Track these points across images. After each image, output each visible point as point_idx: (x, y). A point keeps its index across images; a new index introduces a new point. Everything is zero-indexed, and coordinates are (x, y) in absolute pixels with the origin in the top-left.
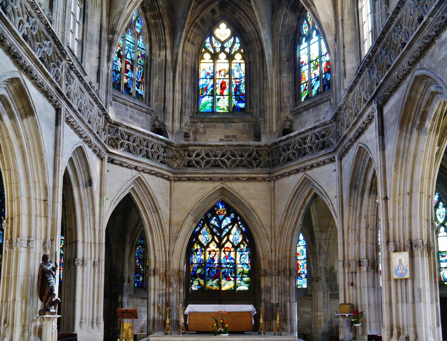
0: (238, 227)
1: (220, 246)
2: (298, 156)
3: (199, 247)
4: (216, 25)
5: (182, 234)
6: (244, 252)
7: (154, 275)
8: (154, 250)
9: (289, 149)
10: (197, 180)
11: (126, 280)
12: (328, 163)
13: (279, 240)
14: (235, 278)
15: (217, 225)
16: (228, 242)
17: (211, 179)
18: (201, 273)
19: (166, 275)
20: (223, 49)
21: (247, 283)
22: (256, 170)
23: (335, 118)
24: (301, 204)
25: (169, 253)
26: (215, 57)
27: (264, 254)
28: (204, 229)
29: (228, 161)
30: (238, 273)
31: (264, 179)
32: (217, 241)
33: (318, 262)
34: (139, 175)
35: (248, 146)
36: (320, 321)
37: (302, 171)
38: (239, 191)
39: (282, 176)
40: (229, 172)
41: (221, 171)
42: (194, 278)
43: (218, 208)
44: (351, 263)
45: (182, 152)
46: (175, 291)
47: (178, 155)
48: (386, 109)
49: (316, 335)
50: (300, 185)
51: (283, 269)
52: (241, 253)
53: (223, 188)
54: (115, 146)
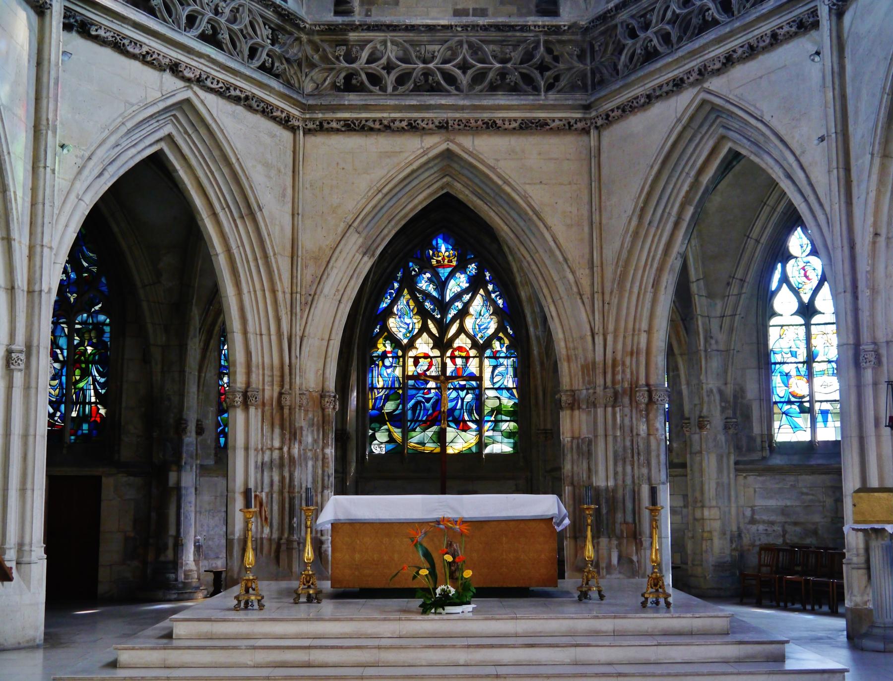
0: (488, 298)
1: (442, 344)
2: (680, 39)
3: (389, 348)
5: (330, 286)
6: (501, 360)
7: (246, 405)
8: (245, 333)
9: (646, 26)
10: (371, 129)
11: (192, 427)
12: (790, 37)
13: (615, 301)
14: (480, 423)
15: (435, 294)
16: (463, 336)
17: (413, 128)
18: (394, 411)
19: (281, 407)
21: (510, 435)
22: (546, 99)
24: (686, 187)
25: (291, 343)
27: (571, 345)
28: (402, 304)
29: (464, 73)
30: (487, 410)
31: (570, 126)
32: (434, 330)
33: (702, 377)
34: (188, 94)
35: (524, 28)
36: (710, 532)
37: (692, 85)
38: (498, 160)
39: (624, 111)
40: (466, 102)
41: (443, 102)
42: (378, 425)
43: (436, 249)
44: (883, 351)
45: (328, 49)
46: (309, 454)
47: (316, 57)
49: (699, 570)
50: (685, 128)
51: (626, 385)
52: (493, 362)
53: (448, 155)
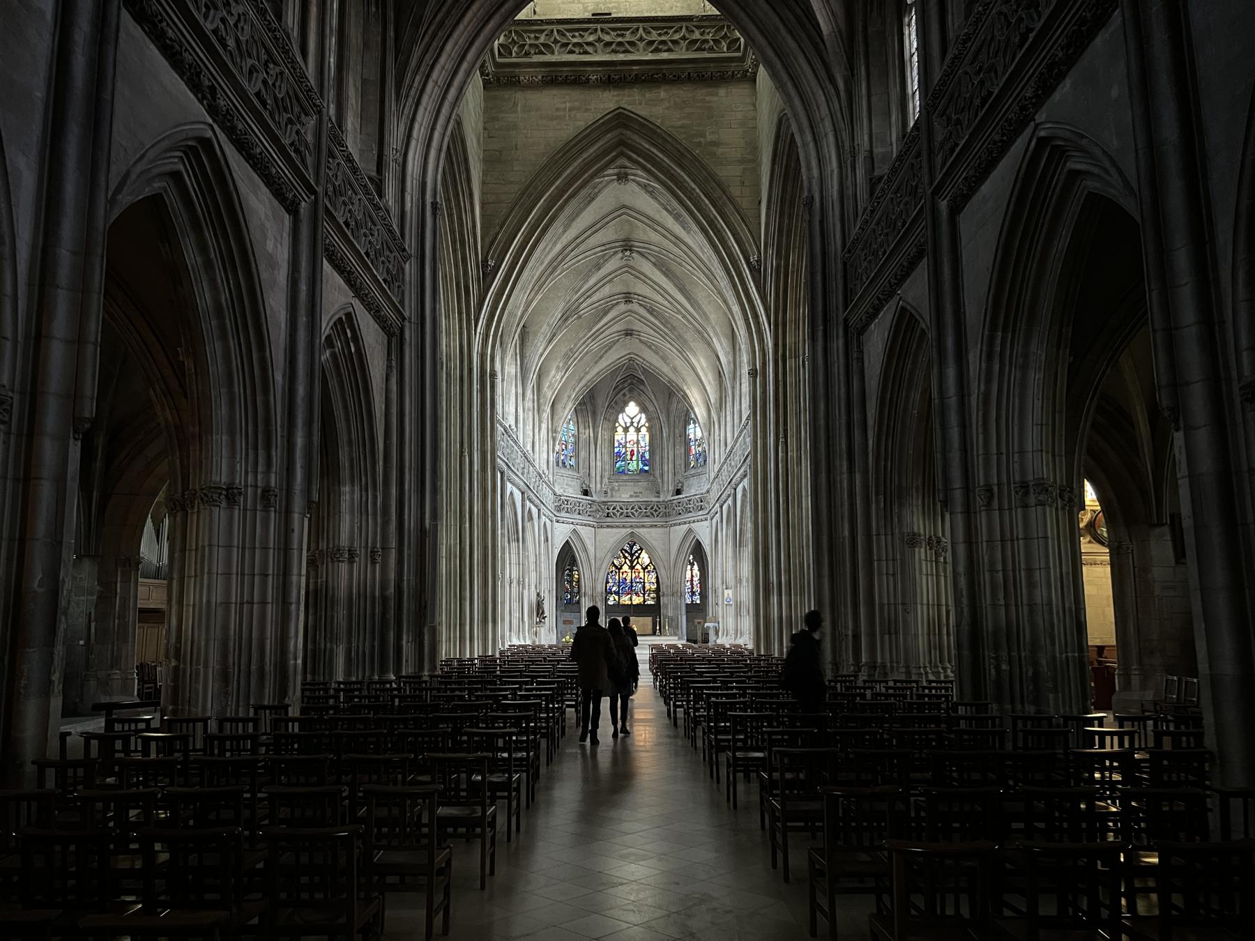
1: (632, 567)
4: (626, 404)
25: (595, 581)
48: (725, 507)
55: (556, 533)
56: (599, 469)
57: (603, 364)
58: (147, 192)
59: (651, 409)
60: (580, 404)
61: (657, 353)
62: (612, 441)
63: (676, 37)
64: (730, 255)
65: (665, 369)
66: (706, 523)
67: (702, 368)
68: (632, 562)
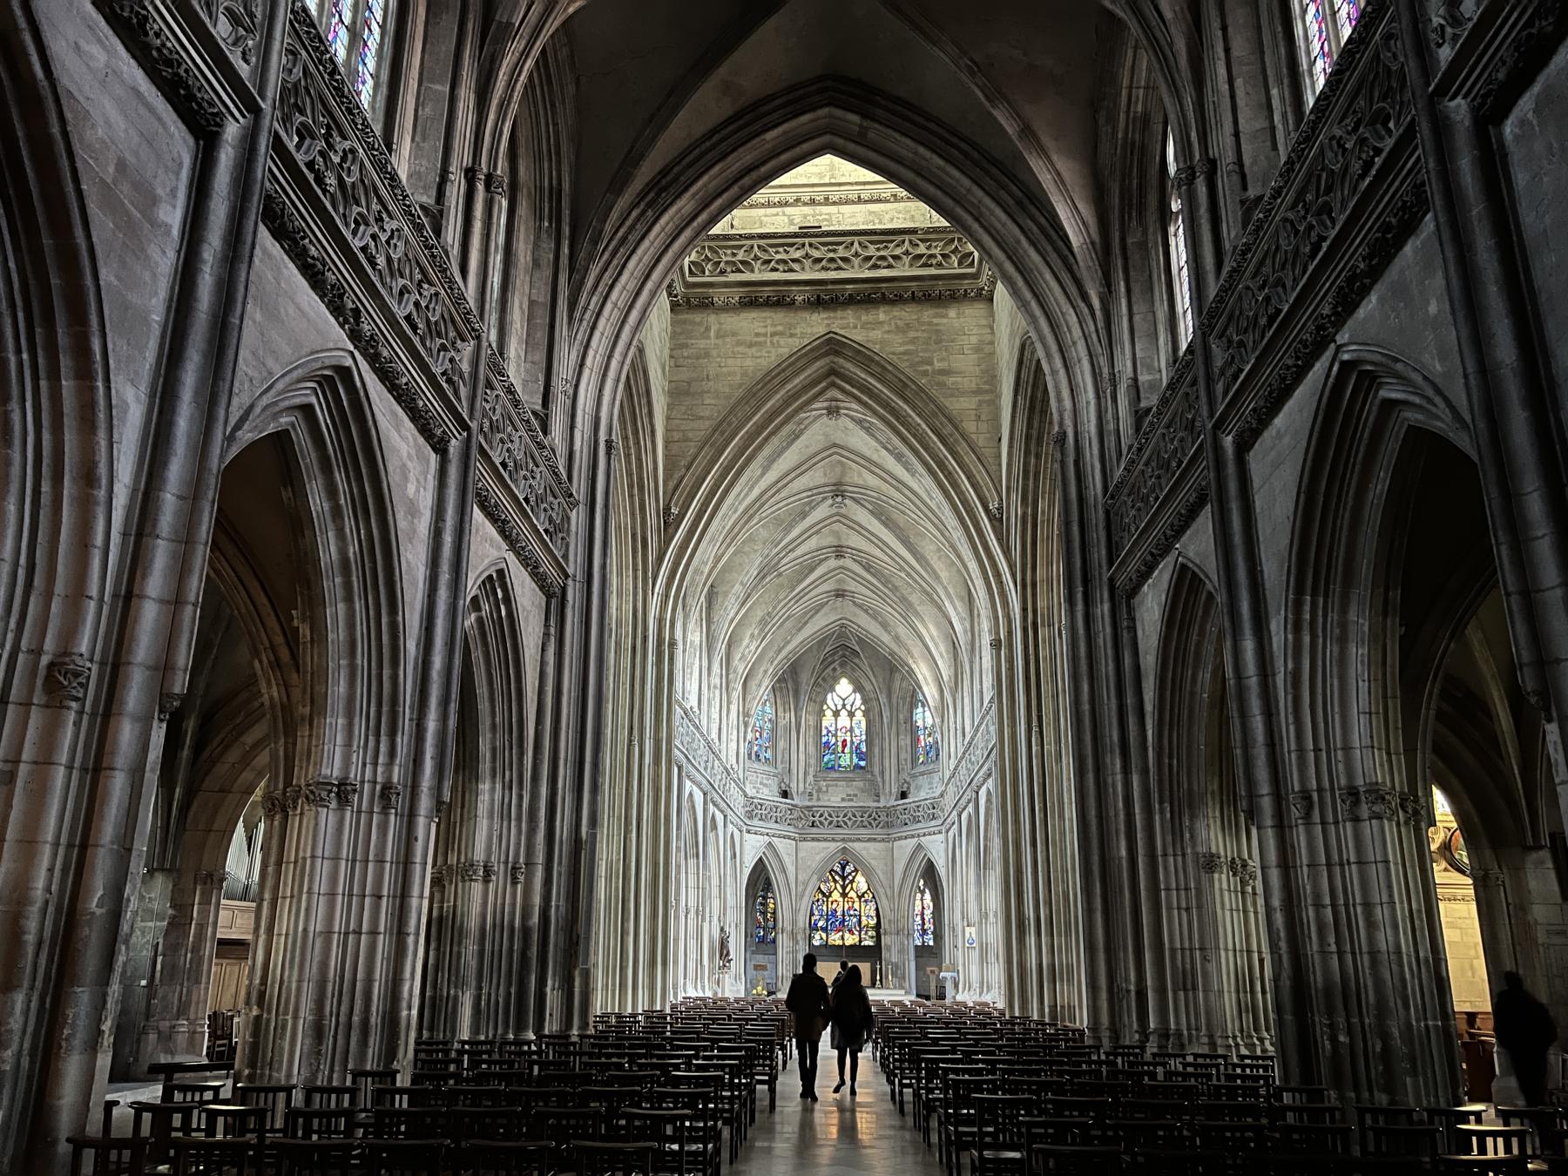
1: (844, 895)
4: (836, 680)
20: (844, 706)
23: (942, 796)
25: (795, 912)
26: (836, 714)
48: (964, 816)
54: (750, 818)
55: (747, 847)
56: (802, 764)
57: (808, 631)
58: (271, 429)
59: (868, 687)
60: (779, 681)
61: (875, 619)
62: (818, 728)
63: (898, 252)
64: (965, 502)
65: (886, 638)
66: (941, 837)
67: (932, 639)
68: (844, 888)
